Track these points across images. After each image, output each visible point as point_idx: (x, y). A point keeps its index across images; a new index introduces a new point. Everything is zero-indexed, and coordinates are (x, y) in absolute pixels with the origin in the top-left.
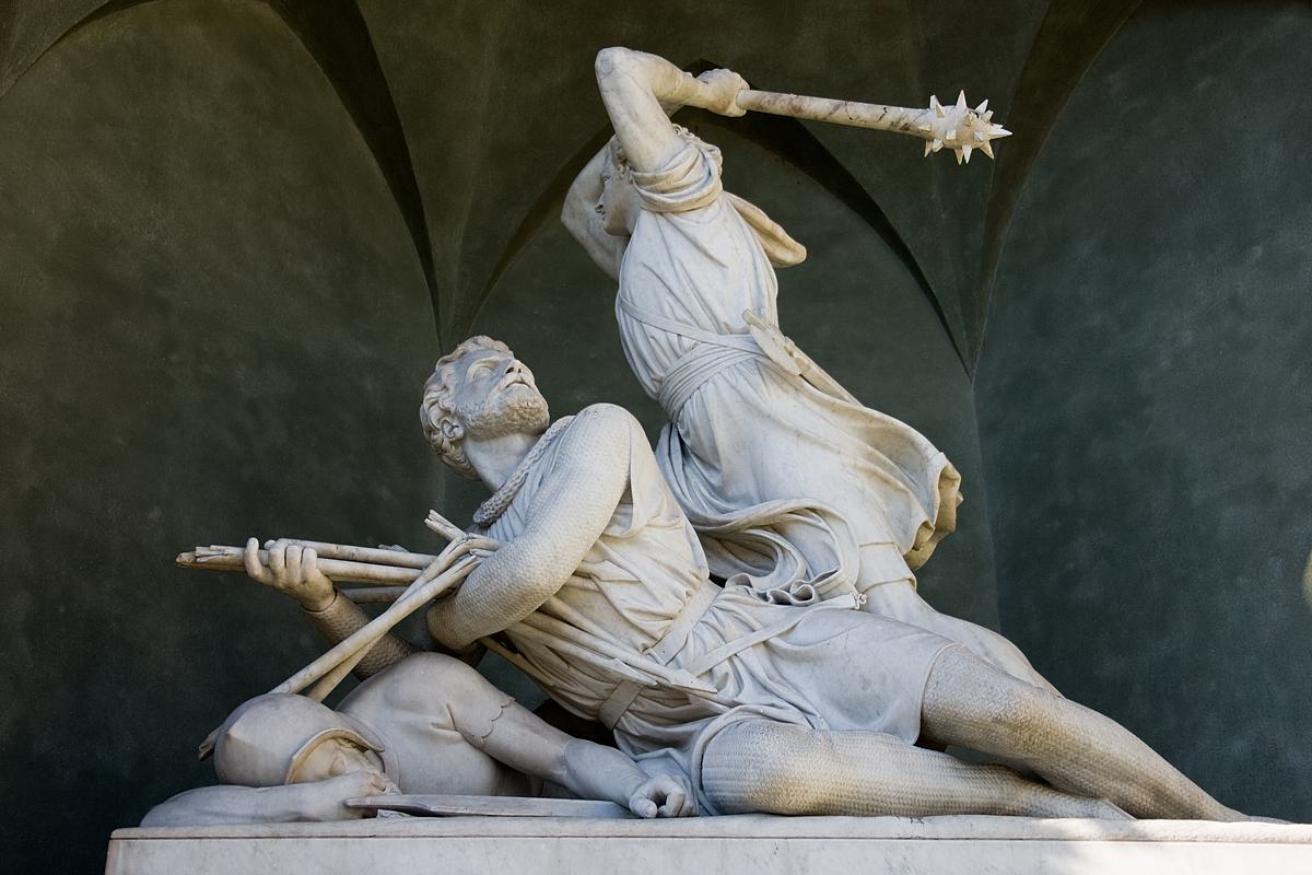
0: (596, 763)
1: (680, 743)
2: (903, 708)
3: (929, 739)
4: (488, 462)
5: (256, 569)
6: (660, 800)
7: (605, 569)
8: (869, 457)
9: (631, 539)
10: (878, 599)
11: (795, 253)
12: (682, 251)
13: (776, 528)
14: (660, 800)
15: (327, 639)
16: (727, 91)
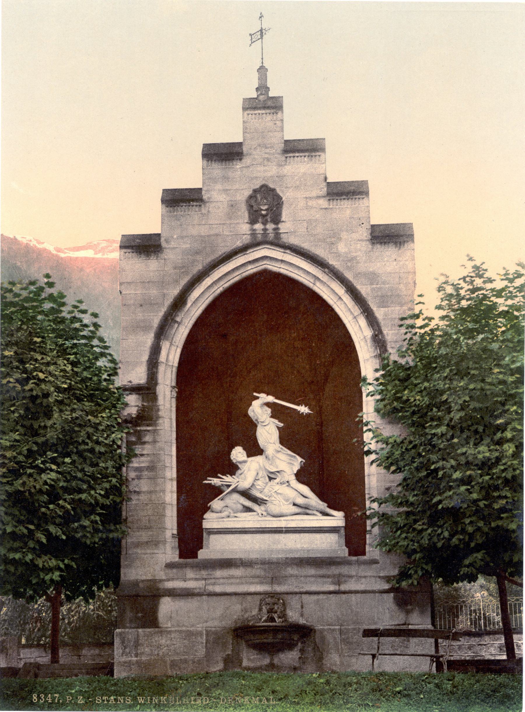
0: (255, 507)
1: (266, 504)
2: (290, 501)
3: (294, 504)
4: (240, 466)
5: (213, 484)
6: (262, 514)
7: (255, 483)
8: (290, 459)
9: (258, 480)
10: (291, 483)
11: (281, 425)
12: (264, 431)
13: (278, 472)
14: (262, 514)
15: (221, 492)
16: (271, 399)
